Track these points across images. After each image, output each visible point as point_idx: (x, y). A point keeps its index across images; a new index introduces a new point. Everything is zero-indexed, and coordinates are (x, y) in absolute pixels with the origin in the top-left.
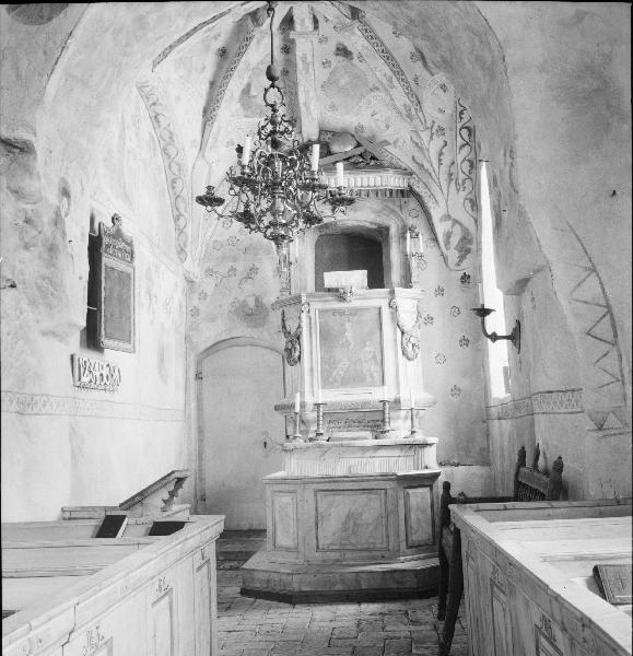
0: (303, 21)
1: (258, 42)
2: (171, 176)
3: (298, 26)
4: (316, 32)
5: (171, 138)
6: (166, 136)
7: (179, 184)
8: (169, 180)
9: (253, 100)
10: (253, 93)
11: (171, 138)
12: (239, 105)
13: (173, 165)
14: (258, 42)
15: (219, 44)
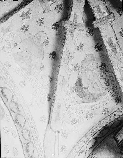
0: (98, 7)
1: (72, 33)
2: (24, 142)
3: (97, 16)
4: (112, 16)
5: (18, 108)
6: (14, 107)
7: (31, 148)
8: (24, 147)
9: (86, 90)
10: (84, 85)
11: (18, 108)
12: (75, 94)
13: (25, 132)
14: (72, 33)
15: (50, 49)
